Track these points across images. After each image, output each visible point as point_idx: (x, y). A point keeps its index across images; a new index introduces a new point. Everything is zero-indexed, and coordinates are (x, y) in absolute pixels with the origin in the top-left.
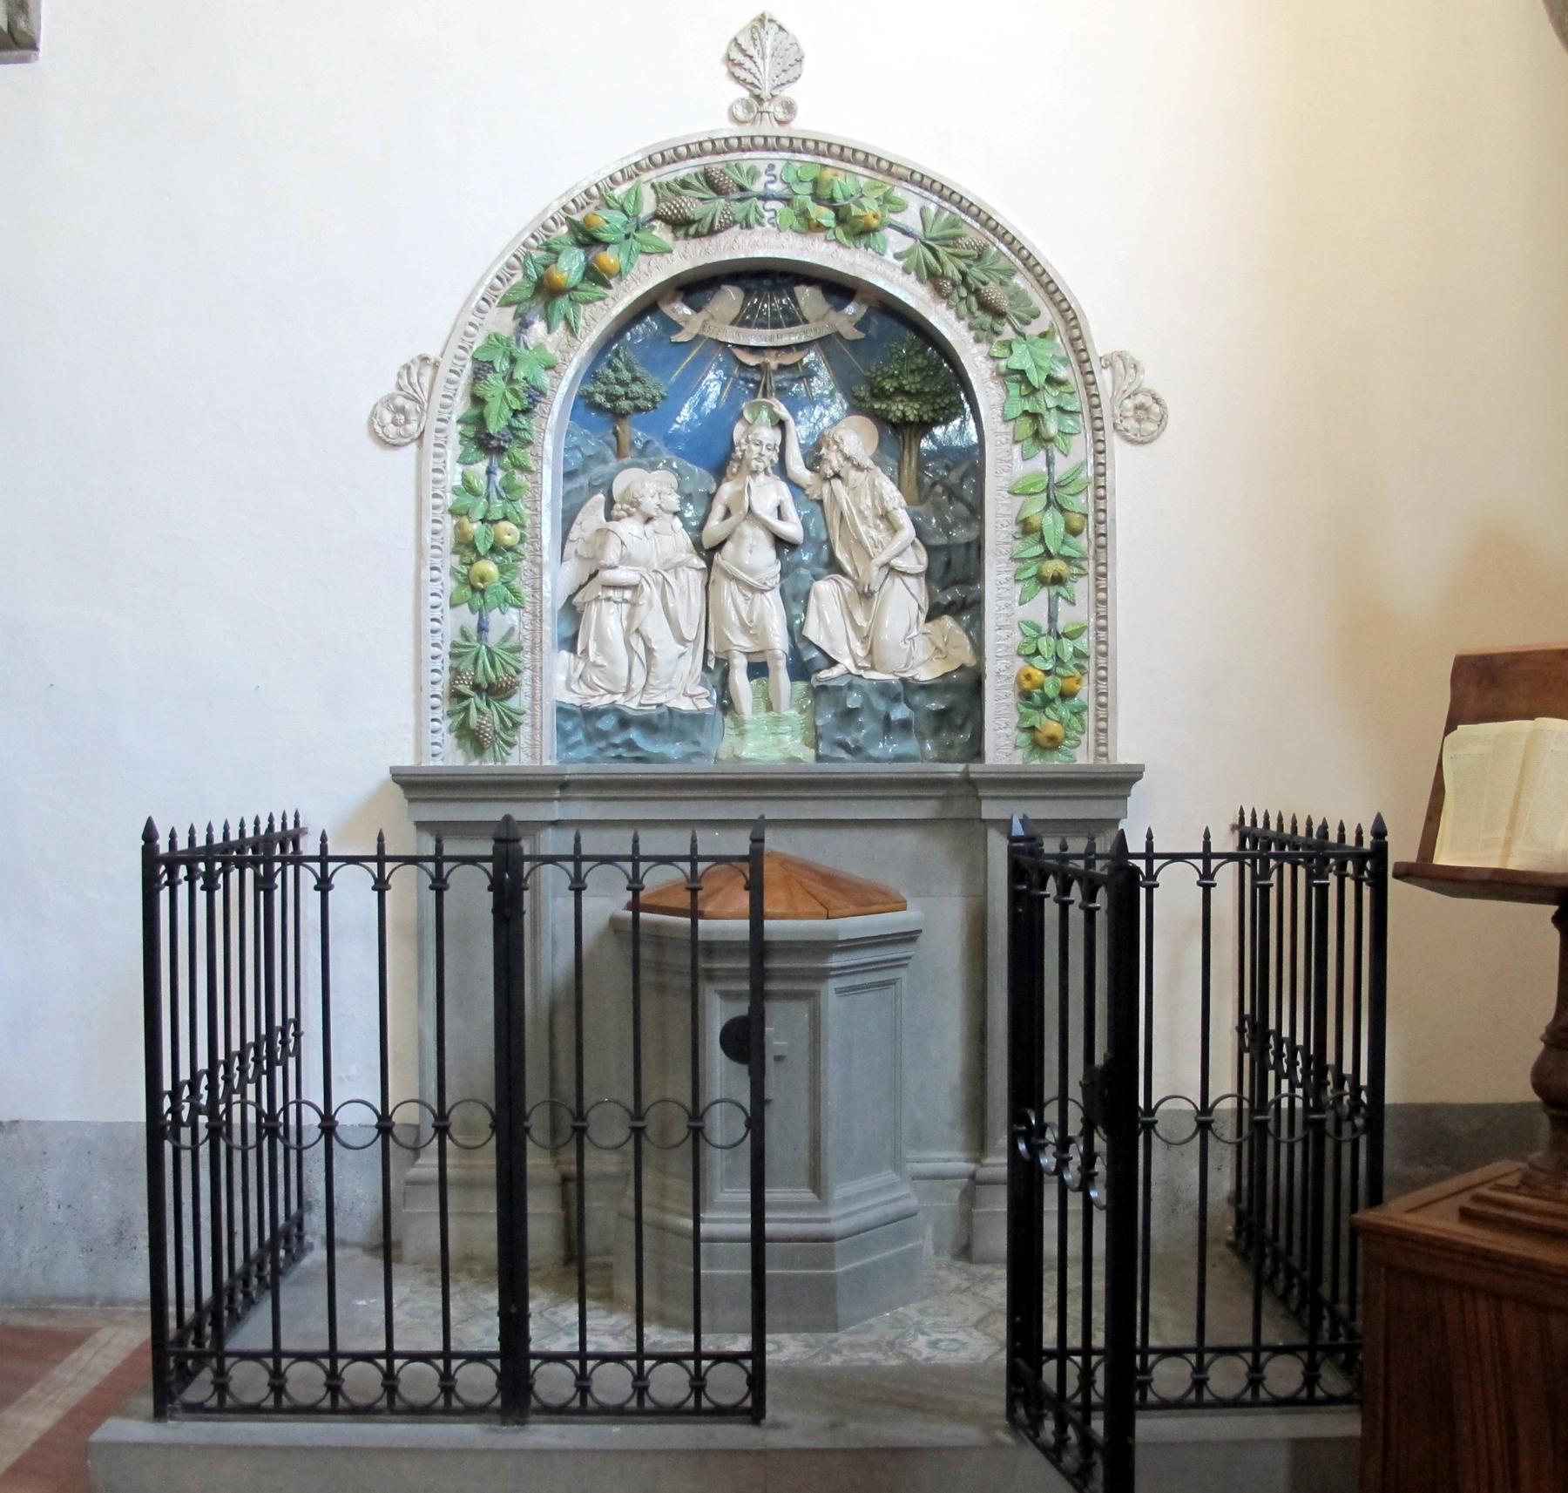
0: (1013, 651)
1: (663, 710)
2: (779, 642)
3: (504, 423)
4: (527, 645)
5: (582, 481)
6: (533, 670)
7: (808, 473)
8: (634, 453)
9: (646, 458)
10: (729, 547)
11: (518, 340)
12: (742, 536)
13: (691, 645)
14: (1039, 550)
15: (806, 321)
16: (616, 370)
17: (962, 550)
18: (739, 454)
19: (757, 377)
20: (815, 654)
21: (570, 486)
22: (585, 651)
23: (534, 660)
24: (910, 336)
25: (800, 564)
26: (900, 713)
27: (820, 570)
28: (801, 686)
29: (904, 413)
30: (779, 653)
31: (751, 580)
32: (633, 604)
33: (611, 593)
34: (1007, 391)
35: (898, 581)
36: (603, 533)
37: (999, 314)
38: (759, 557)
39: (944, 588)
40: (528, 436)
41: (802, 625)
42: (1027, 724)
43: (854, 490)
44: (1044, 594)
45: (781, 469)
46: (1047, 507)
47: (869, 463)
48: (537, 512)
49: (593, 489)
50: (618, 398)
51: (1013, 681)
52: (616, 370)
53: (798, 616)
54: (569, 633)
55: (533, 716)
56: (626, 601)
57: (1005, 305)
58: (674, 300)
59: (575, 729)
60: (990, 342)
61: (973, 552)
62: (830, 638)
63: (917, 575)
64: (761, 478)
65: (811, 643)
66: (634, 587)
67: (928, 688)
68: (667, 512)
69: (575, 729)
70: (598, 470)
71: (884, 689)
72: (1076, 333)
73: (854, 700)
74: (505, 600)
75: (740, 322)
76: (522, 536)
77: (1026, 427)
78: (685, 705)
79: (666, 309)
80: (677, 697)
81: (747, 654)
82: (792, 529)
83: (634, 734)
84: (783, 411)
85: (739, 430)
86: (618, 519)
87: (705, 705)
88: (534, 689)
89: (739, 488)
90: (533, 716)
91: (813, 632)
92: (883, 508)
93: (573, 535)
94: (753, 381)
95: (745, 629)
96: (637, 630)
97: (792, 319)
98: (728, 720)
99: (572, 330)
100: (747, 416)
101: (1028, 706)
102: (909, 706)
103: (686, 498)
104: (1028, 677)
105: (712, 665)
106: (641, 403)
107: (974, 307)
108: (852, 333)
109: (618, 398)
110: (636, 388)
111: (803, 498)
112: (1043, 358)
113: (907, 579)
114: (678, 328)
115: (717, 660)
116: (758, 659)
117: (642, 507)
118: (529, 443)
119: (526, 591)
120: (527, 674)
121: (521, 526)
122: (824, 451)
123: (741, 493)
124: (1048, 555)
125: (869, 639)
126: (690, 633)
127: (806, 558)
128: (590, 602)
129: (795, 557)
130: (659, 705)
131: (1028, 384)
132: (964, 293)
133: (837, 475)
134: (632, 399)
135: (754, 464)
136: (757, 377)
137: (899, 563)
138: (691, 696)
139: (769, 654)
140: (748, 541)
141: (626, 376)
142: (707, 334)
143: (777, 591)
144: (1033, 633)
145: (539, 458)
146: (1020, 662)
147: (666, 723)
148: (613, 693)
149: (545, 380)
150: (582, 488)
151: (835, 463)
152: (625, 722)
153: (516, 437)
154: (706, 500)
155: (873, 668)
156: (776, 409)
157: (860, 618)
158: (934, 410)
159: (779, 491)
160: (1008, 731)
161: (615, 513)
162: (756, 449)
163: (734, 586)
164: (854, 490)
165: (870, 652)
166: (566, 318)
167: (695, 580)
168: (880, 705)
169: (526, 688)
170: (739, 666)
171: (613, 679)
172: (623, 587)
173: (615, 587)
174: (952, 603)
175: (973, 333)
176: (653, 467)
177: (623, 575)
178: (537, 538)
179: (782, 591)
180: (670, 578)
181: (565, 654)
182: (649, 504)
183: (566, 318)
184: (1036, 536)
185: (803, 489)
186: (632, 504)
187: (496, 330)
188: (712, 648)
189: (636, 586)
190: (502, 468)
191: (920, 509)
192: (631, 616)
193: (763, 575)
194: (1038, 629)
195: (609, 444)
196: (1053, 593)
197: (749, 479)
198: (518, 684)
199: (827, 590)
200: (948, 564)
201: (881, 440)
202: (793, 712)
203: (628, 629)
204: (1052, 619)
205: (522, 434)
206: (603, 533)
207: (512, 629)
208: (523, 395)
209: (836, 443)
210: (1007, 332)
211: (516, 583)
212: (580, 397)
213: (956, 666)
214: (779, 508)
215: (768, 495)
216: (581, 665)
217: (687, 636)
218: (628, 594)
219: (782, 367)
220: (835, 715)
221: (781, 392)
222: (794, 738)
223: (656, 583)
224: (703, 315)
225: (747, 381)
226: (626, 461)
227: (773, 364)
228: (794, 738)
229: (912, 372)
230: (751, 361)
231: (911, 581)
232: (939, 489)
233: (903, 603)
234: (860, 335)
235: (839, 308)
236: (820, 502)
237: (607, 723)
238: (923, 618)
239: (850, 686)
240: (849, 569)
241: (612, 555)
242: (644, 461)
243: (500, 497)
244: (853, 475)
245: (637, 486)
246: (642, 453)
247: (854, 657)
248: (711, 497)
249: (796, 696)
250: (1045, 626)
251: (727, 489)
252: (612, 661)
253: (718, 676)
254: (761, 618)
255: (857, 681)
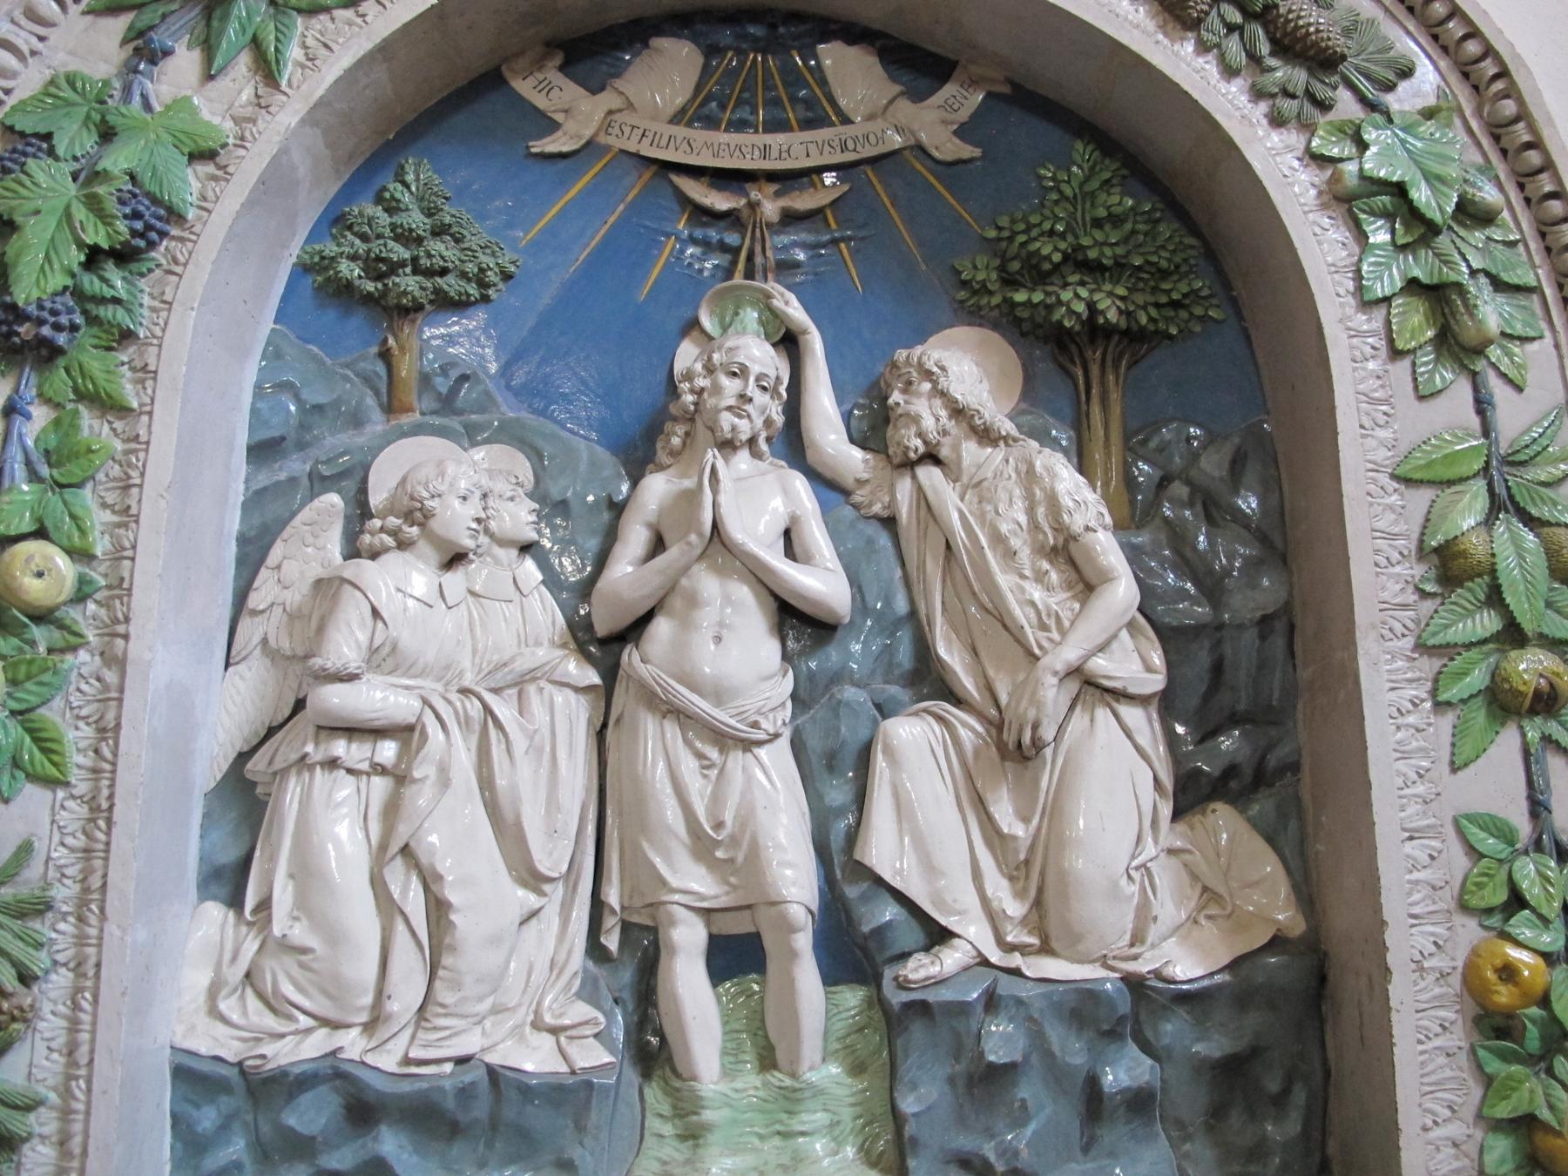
0: (1447, 899)
1: (476, 1074)
2: (795, 881)
3: (58, 280)
4: (64, 893)
5: (297, 465)
6: (78, 968)
7: (857, 454)
8: (428, 403)
9: (454, 409)
10: (661, 628)
11: (127, 90)
12: (693, 601)
13: (557, 892)
14: (1488, 623)
15: (846, 120)
16: (392, 208)
17: (1250, 635)
18: (689, 398)
19: (732, 239)
20: (889, 912)
21: (263, 479)
22: (265, 905)
23: (81, 940)
24: (1081, 150)
25: (839, 677)
26: (1124, 1071)
27: (894, 690)
28: (852, 997)
29: (1091, 306)
30: (798, 914)
31: (722, 716)
32: (400, 777)
33: (340, 748)
34: (1361, 236)
35: (1103, 714)
36: (328, 589)
37: (1324, 61)
38: (735, 653)
39: (1206, 735)
40: (121, 315)
41: (852, 837)
42: (1503, 1111)
43: (977, 488)
44: (1508, 742)
45: (792, 441)
46: (1489, 522)
47: (1008, 427)
48: (127, 516)
49: (319, 483)
50: (395, 267)
51: (1456, 980)
52: (392, 208)
53: (840, 812)
54: (229, 854)
55: (66, 1114)
56: (379, 769)
57: (1339, 43)
58: (539, 64)
59: (224, 1127)
60: (1309, 128)
61: (1278, 643)
62: (930, 868)
63: (1141, 700)
64: (743, 460)
65: (879, 881)
66: (405, 733)
67: (1192, 1000)
68: (503, 543)
69: (224, 1127)
70: (335, 441)
71: (1081, 1007)
72: (1509, 108)
73: (1001, 1040)
74: (16, 763)
75: (699, 112)
76: (82, 581)
77: (1415, 323)
78: (535, 1058)
79: (524, 87)
80: (517, 1031)
81: (707, 913)
82: (822, 582)
83: (390, 1143)
84: (795, 311)
85: (687, 355)
86: (374, 556)
87: (591, 1055)
88: (74, 1026)
89: (689, 483)
90: (66, 1114)
91: (884, 850)
92: (1059, 527)
93: (255, 600)
94: (723, 248)
95: (702, 846)
96: (406, 850)
97: (818, 112)
98: (653, 1093)
99: (267, 70)
100: (707, 322)
101: (1505, 1057)
102: (1147, 1048)
103: (553, 508)
104: (1508, 972)
105: (612, 942)
106: (451, 284)
107: (1264, 48)
108: (948, 147)
109: (395, 267)
110: (441, 249)
111: (848, 511)
112: (1445, 159)
113: (1126, 711)
114: (554, 126)
115: (626, 927)
116: (737, 925)
117: (434, 524)
118: (127, 336)
119: (76, 738)
120: (61, 980)
121: (80, 554)
122: (896, 397)
123: (690, 499)
124: (1513, 635)
125: (1038, 874)
126: (550, 856)
127: (867, 660)
128: (284, 773)
129: (832, 655)
130: (461, 1061)
131: (1414, 215)
132: (1235, 17)
133: (932, 457)
134: (429, 273)
135: (727, 420)
136: (732, 239)
137: (1100, 665)
138: (555, 1031)
139: (764, 915)
140: (707, 618)
141: (416, 219)
142: (615, 142)
143: (784, 743)
144: (1489, 844)
145: (145, 373)
146: (1470, 931)
147: (481, 1109)
148: (336, 1026)
149: (189, 184)
150: (293, 481)
151: (928, 423)
152: (363, 1108)
153: (93, 320)
154: (606, 516)
155: (1046, 949)
156: (777, 303)
157: (1004, 813)
158: (1157, 305)
159: (787, 492)
160: (1456, 1130)
161: (367, 539)
162: (731, 386)
163: (672, 729)
164: (977, 488)
165: (1038, 904)
166: (256, 43)
167: (570, 716)
168: (1073, 1050)
169: (51, 1025)
170: (688, 942)
171: (334, 987)
172: (377, 733)
173: (353, 731)
174: (1231, 771)
175: (1263, 107)
176: (471, 436)
177: (375, 698)
178: (121, 588)
179: (798, 747)
180: (504, 710)
181: (215, 911)
182: (456, 519)
183: (256, 43)
184: (1479, 587)
185: (846, 493)
186: (408, 517)
187: (74, 65)
188: (613, 897)
189: (410, 728)
190: (48, 401)
191: (1140, 539)
192: (392, 810)
193: (750, 704)
194: (1505, 833)
195: (368, 380)
196: (1532, 735)
197: (712, 456)
198: (24, 1016)
199: (914, 740)
200: (1218, 669)
201: (1028, 379)
202: (834, 1069)
203: (383, 847)
204: (1538, 807)
205: (106, 312)
206: (328, 589)
207: (25, 850)
208: (112, 206)
209: (928, 375)
210: (1346, 105)
211: (52, 714)
212: (304, 268)
213: (1263, 939)
214: (787, 533)
215: (760, 502)
216: (251, 946)
217: (544, 867)
218: (388, 751)
219: (790, 218)
220: (951, 1080)
221: (785, 268)
222: (839, 1143)
223: (465, 723)
224: (608, 100)
225: (706, 244)
226: (406, 420)
227: (770, 209)
228: (839, 1143)
229: (1098, 223)
230: (721, 202)
231: (1134, 715)
232: (1180, 490)
233: (1114, 776)
234: (968, 151)
235: (918, 96)
236: (889, 522)
237: (311, 1115)
238: (1166, 810)
239: (991, 1002)
240: (968, 683)
241: (346, 643)
242: (454, 423)
243: (34, 476)
244: (971, 452)
245: (428, 471)
246: (447, 404)
247: (994, 917)
248: (617, 509)
249: (840, 1026)
250: (1523, 827)
251: (657, 488)
252: (334, 936)
253: (627, 975)
254: (746, 817)
255: (1006, 986)
